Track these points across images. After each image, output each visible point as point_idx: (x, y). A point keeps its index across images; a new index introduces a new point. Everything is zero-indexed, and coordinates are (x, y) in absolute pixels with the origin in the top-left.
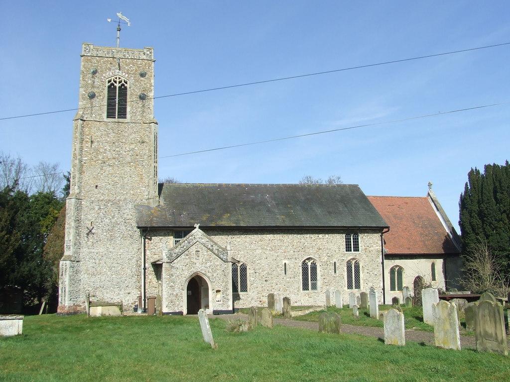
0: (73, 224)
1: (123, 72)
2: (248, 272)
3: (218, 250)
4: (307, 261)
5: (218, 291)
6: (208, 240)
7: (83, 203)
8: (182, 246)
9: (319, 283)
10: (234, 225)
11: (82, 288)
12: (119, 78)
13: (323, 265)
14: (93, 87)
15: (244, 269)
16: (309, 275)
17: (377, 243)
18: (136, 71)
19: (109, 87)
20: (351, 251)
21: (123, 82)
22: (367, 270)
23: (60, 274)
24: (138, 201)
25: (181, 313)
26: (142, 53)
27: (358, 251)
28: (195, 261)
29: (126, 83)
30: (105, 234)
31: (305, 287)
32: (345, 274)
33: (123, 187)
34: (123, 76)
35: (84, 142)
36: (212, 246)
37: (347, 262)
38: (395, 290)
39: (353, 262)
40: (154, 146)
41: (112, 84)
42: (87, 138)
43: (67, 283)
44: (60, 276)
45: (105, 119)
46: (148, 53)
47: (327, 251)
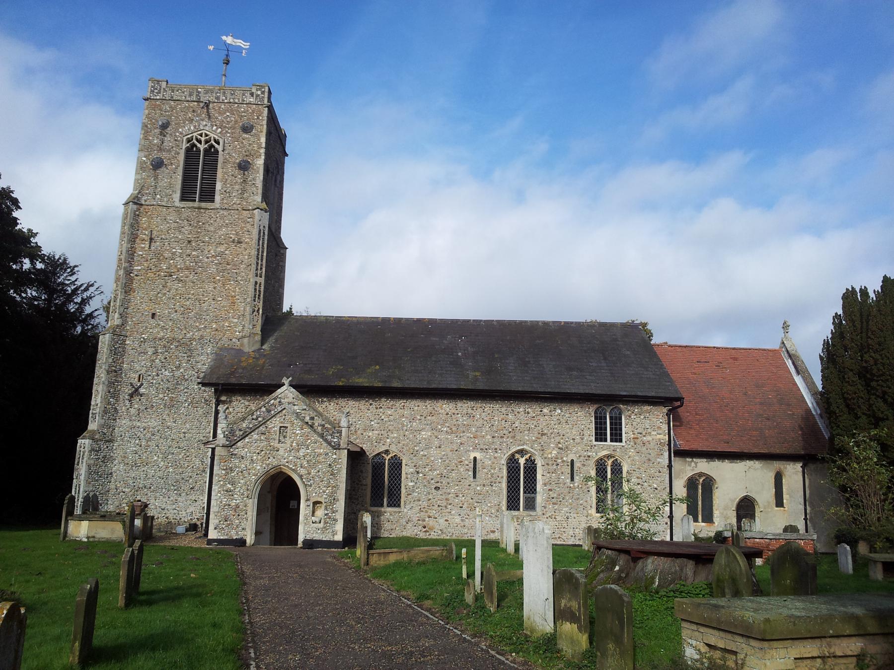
1: (212, 126)
2: (404, 470)
3: (323, 426)
4: (517, 456)
7: (128, 342)
8: (254, 417)
9: (540, 499)
10: (380, 385)
11: (113, 487)
14: (160, 150)
16: (521, 483)
17: (659, 428)
18: (236, 122)
19: (188, 150)
20: (606, 440)
22: (638, 478)
24: (225, 342)
25: (242, 542)
26: (248, 94)
27: (621, 441)
28: (277, 445)
29: (218, 143)
30: (161, 396)
31: (513, 504)
33: (199, 317)
35: (138, 241)
36: (312, 418)
37: (597, 461)
39: (610, 462)
40: (257, 247)
41: (194, 145)
42: (144, 235)
43: (82, 477)
45: (177, 203)
47: (558, 439)
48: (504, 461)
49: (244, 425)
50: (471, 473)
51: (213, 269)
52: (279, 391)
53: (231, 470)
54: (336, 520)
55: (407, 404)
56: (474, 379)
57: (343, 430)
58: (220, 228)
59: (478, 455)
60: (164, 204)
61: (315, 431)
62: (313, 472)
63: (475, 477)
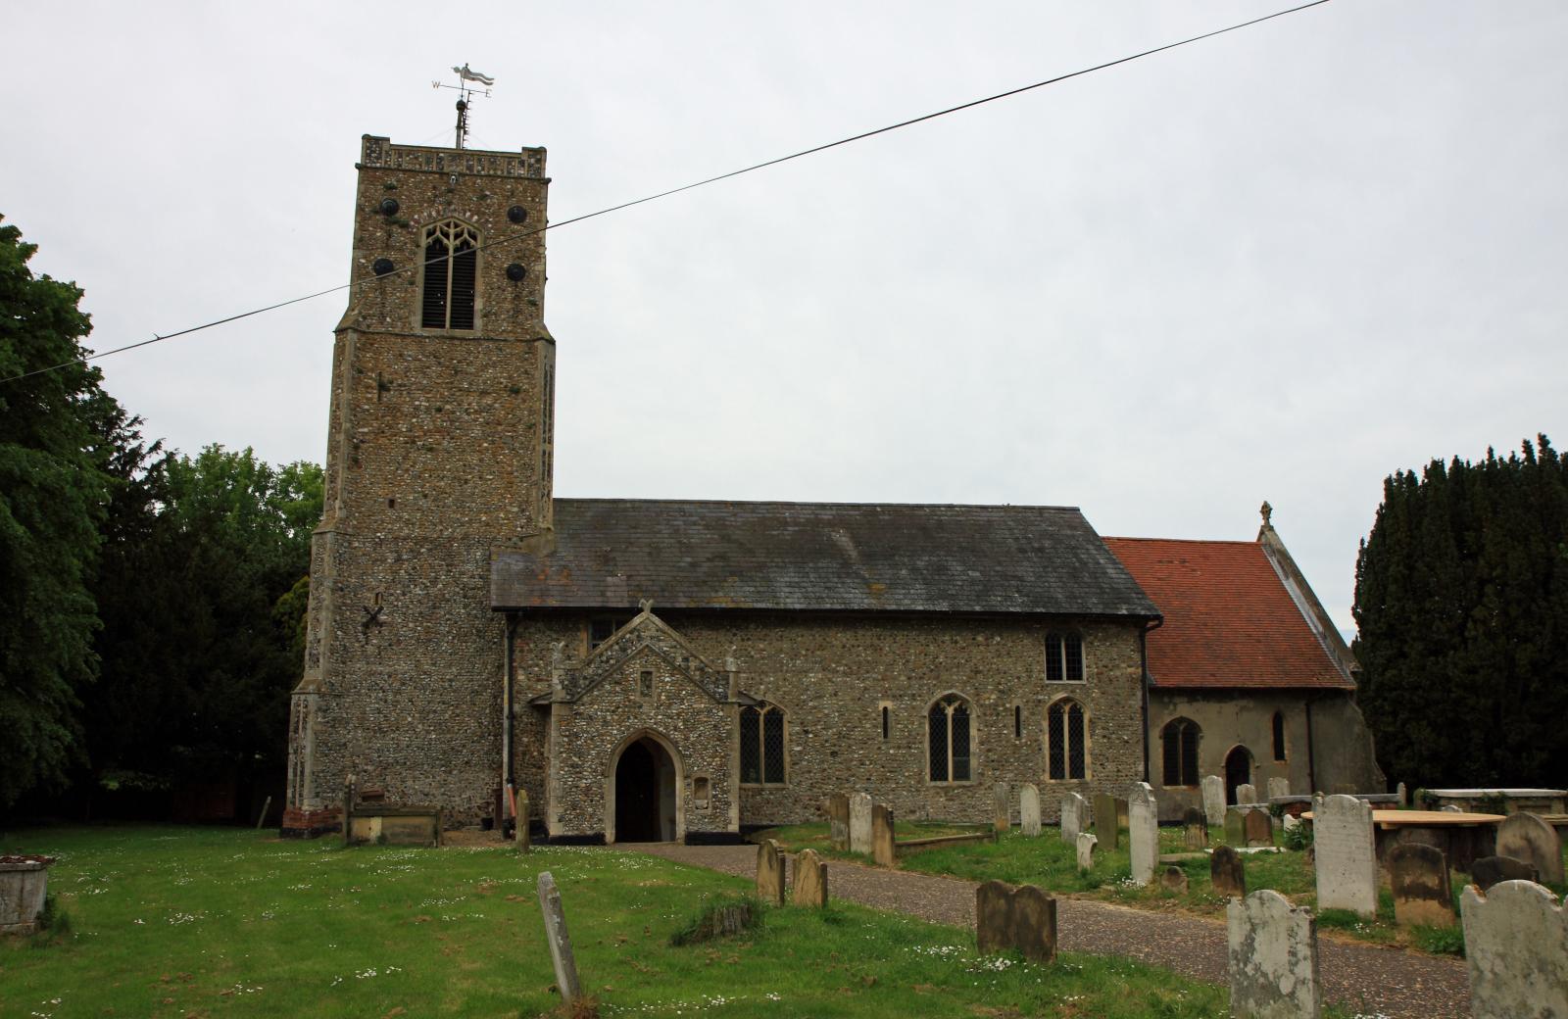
0: (326, 597)
2: (788, 730)
4: (943, 704)
5: (701, 782)
6: (674, 643)
8: (604, 658)
12: (456, 226)
13: (985, 715)
14: (388, 247)
15: (775, 719)
16: (947, 739)
17: (1130, 658)
18: (500, 205)
20: (1060, 678)
21: (466, 235)
22: (1103, 728)
23: (291, 728)
31: (938, 773)
32: (1046, 738)
33: (460, 505)
34: (470, 220)
35: (361, 389)
36: (686, 659)
39: (1067, 708)
40: (543, 398)
41: (438, 241)
43: (308, 750)
44: (291, 734)
45: (418, 330)
46: (532, 161)
47: (997, 678)
48: (926, 714)
49: (590, 671)
51: (477, 432)
52: (637, 620)
53: (577, 736)
54: (728, 804)
55: (786, 634)
57: (731, 675)
58: (485, 367)
59: (889, 704)
60: (397, 331)
61: (691, 680)
62: (693, 737)
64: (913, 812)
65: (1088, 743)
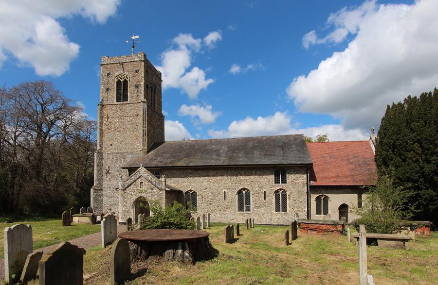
2: (198, 197)
10: (185, 165)
14: (108, 83)
16: (244, 200)
20: (279, 183)
27: (286, 183)
32: (274, 201)
36: (152, 179)
38: (321, 214)
41: (119, 80)
42: (105, 116)
50: (223, 198)
52: (139, 169)
56: (223, 161)
59: (226, 191)
63: (225, 199)
64: (233, 220)
65: (288, 202)
